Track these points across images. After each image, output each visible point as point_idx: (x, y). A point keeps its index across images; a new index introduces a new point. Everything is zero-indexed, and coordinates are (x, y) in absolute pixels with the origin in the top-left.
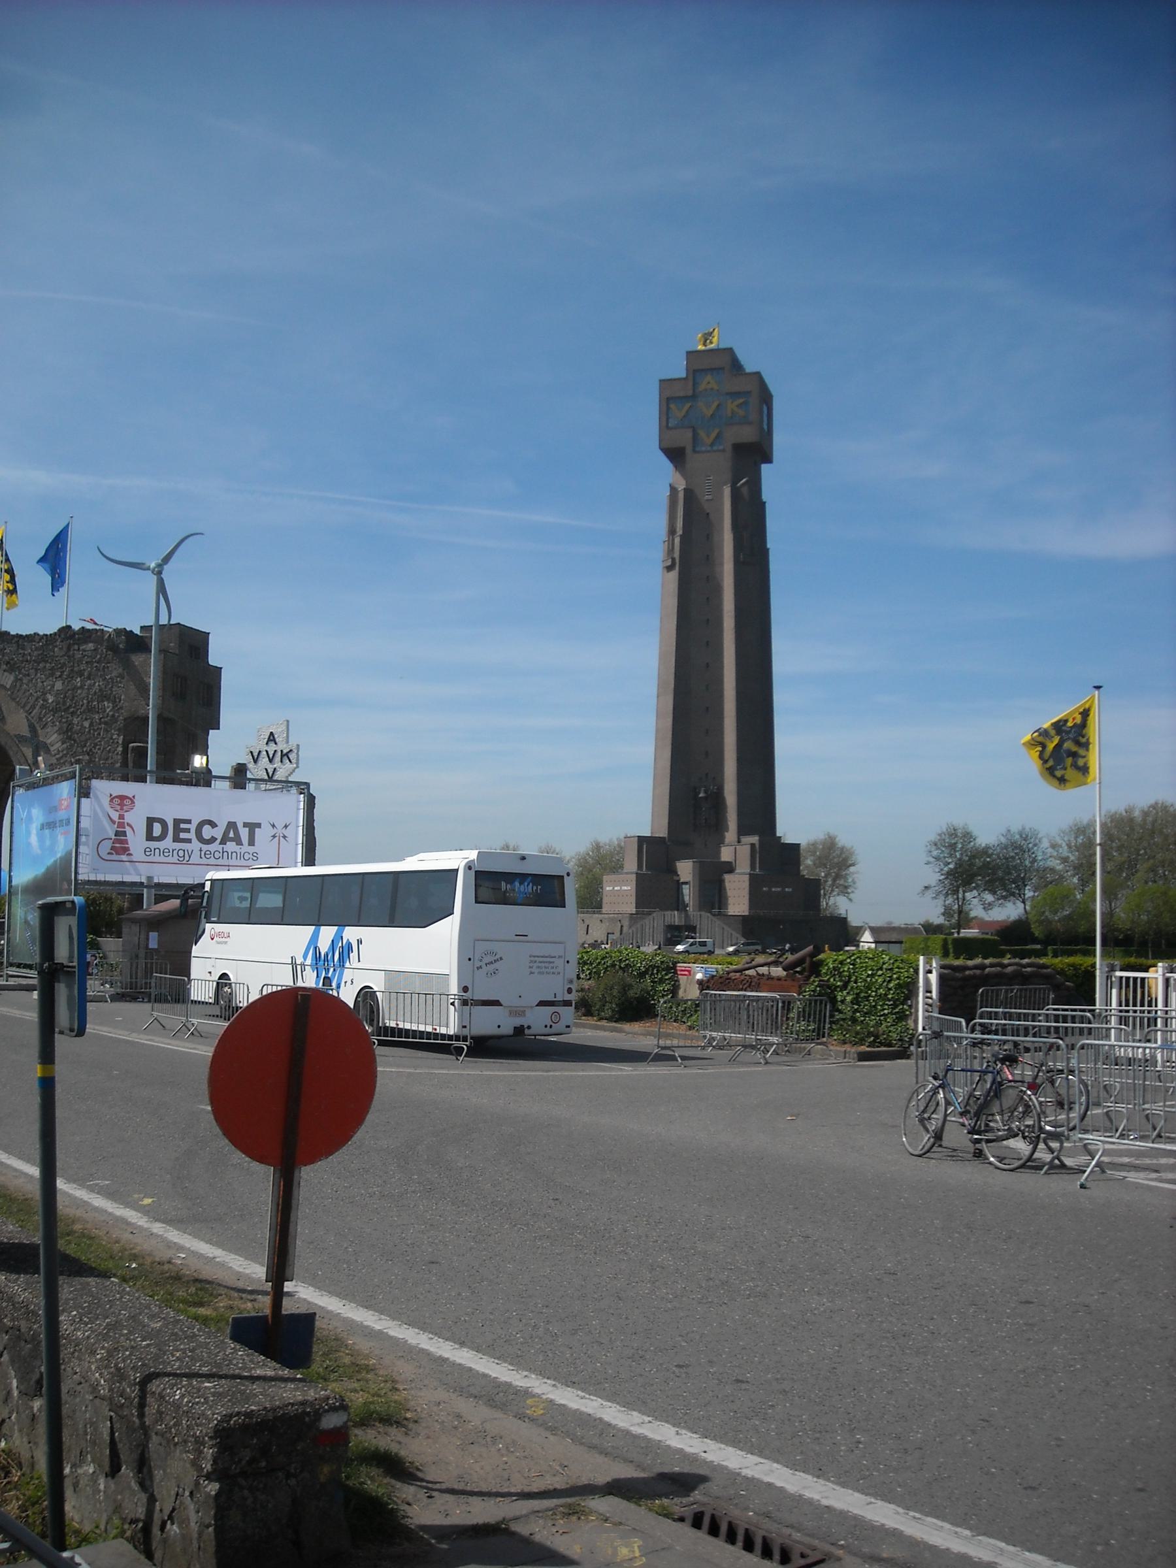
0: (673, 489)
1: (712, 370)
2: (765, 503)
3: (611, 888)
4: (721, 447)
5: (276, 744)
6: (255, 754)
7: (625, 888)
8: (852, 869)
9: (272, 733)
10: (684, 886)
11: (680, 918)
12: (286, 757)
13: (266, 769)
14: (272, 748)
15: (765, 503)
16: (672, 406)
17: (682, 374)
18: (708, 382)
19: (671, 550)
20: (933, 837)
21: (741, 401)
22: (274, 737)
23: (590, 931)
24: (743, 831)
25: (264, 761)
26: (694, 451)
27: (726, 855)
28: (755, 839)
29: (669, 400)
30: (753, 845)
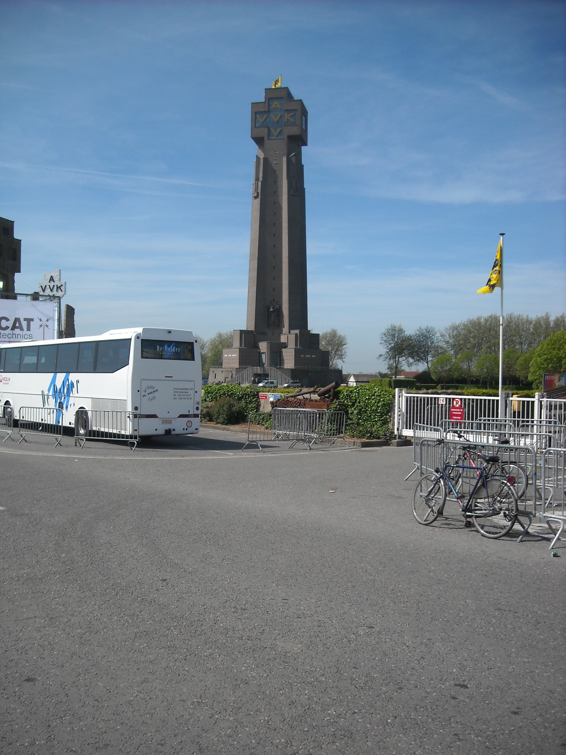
0: (258, 158)
1: (277, 98)
2: (303, 165)
3: (227, 356)
4: (282, 137)
5: (54, 282)
6: (44, 287)
7: (234, 355)
8: (344, 346)
9: (52, 276)
10: (262, 354)
11: (261, 370)
12: (59, 289)
14: (52, 284)
15: (303, 165)
16: (258, 116)
17: (263, 100)
18: (275, 104)
19: (256, 189)
20: (384, 331)
21: (293, 114)
22: (53, 278)
23: (216, 377)
24: (291, 327)
26: (268, 139)
27: (283, 339)
28: (297, 331)
29: (256, 113)
30: (296, 334)
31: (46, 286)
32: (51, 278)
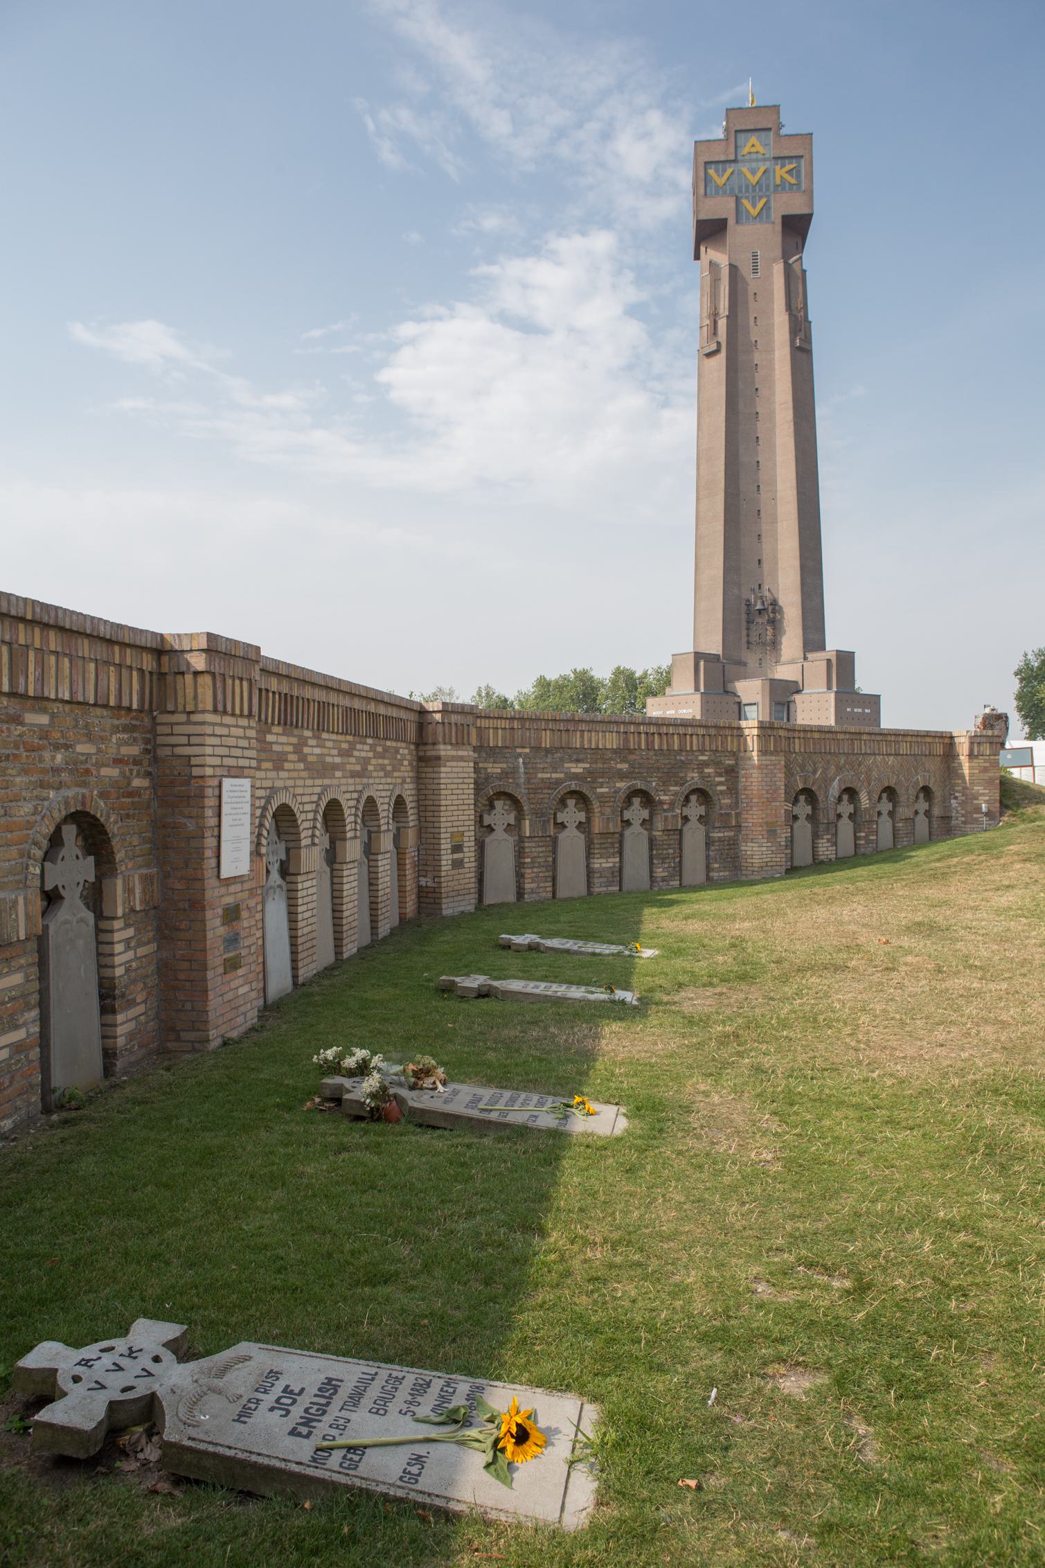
10: (747, 708)
16: (711, 172)
21: (792, 166)
26: (737, 222)
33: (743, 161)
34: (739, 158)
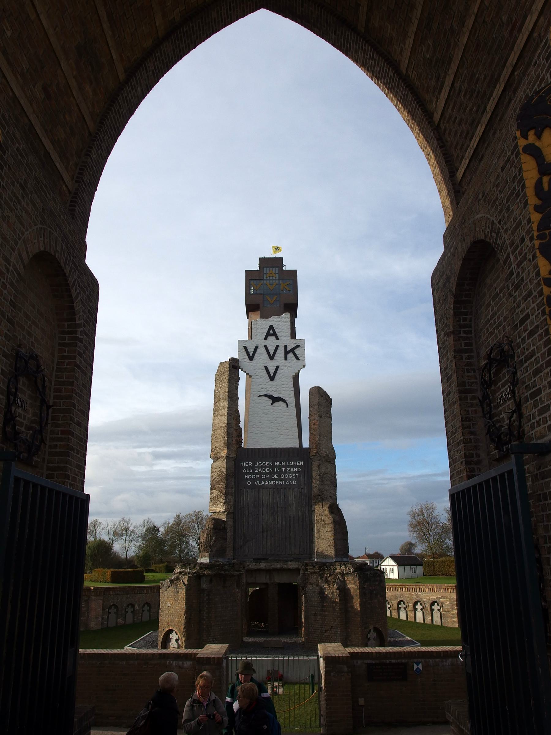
5: (277, 338)
6: (251, 352)
13: (266, 368)
14: (272, 343)
25: (262, 358)
31: (257, 347)
32: (269, 331)
33: (267, 280)
34: (265, 278)
